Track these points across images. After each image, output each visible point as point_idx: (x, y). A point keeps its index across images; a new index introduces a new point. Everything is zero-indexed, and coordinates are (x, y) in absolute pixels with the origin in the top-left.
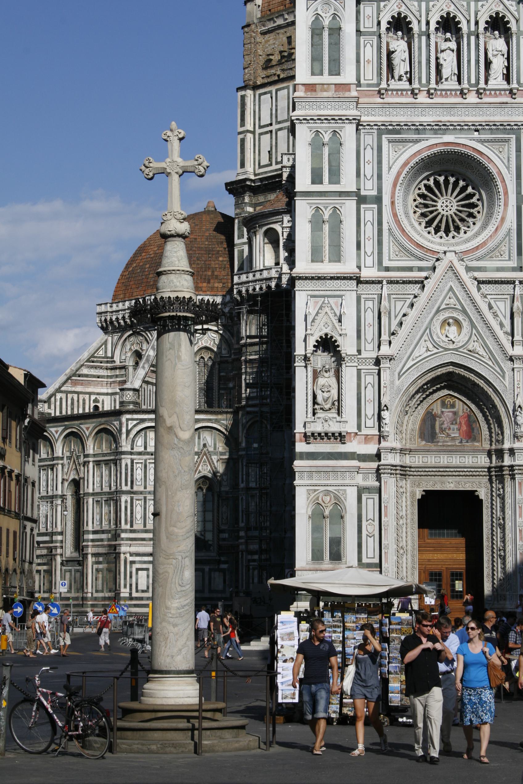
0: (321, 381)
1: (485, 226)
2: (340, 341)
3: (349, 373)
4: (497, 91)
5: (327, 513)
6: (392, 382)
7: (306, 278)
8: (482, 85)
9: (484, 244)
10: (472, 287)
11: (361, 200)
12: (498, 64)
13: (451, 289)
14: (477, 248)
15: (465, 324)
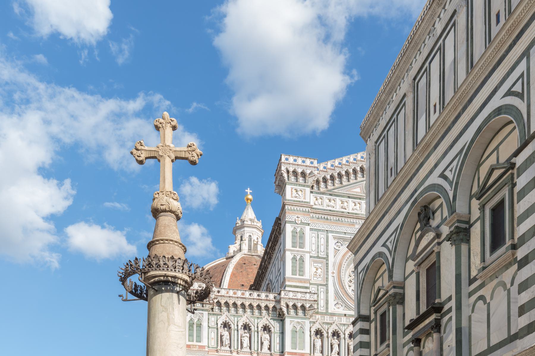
8: (259, 350)
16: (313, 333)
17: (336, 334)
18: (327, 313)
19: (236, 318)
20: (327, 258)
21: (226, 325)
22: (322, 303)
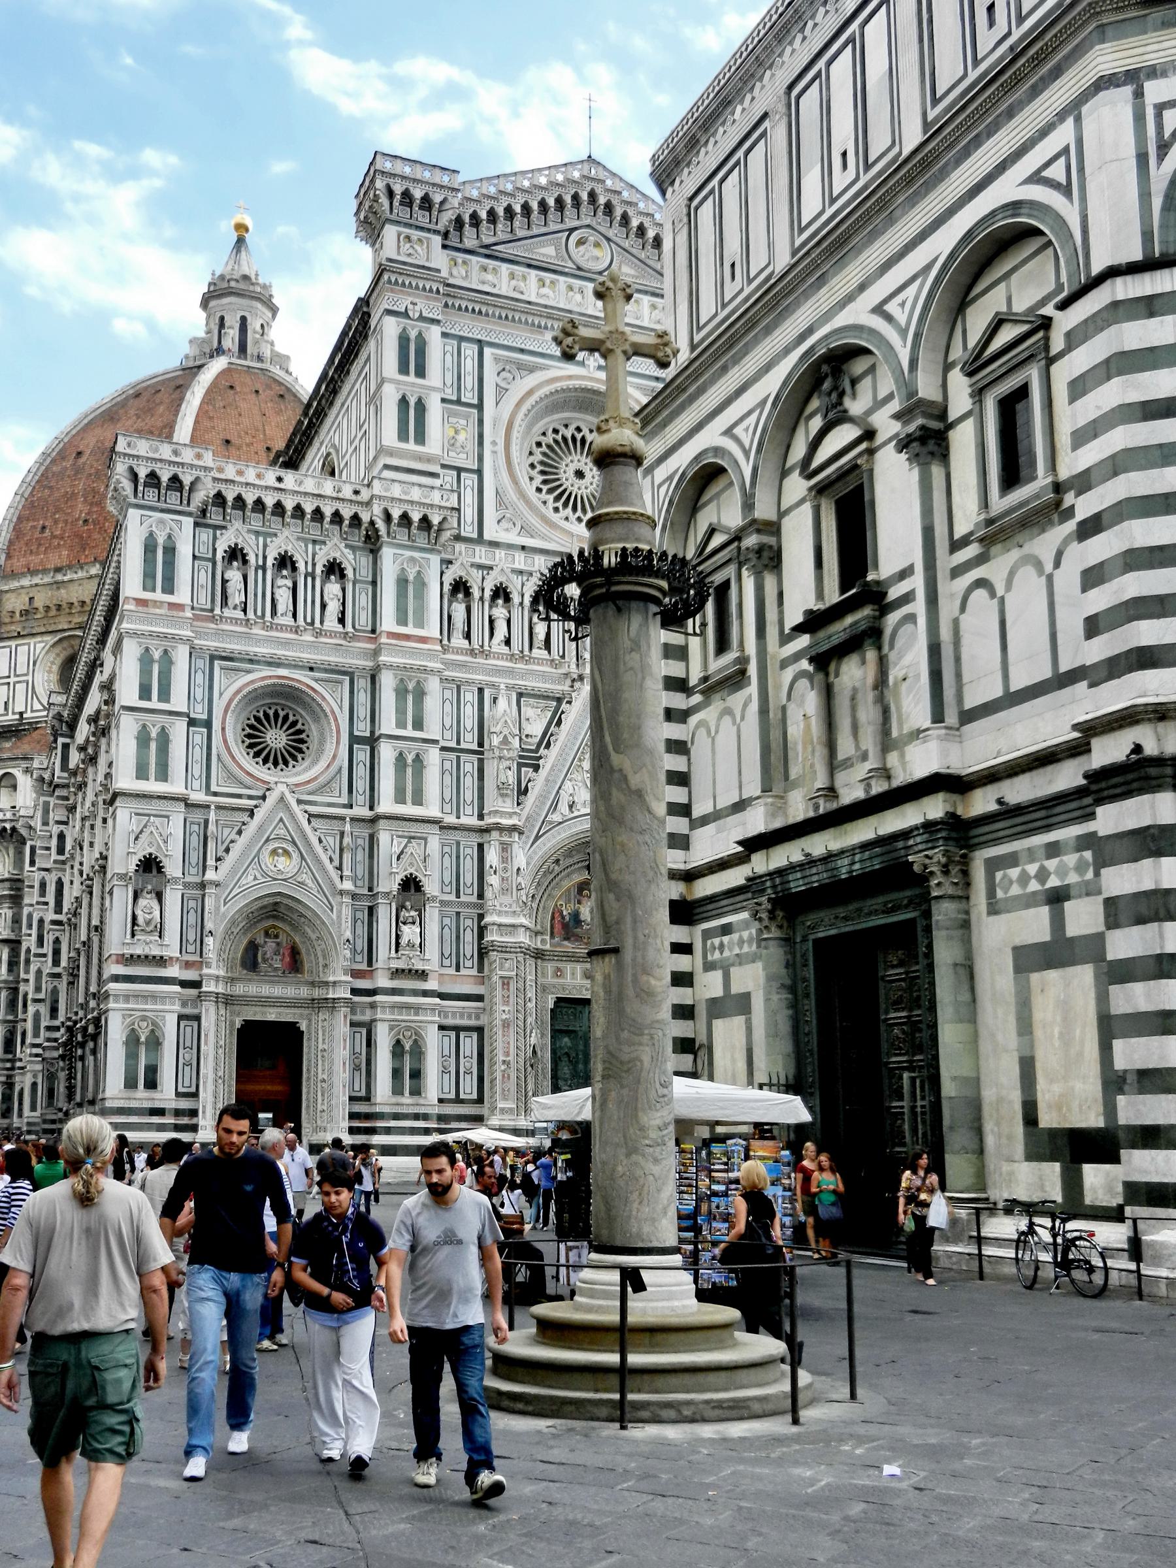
0: (142, 902)
1: (315, 762)
2: (166, 862)
3: (173, 897)
4: (332, 634)
5: (143, 1039)
6: (217, 908)
7: (130, 795)
9: (316, 778)
10: (303, 819)
11: (192, 723)
12: (333, 607)
13: (281, 820)
14: (308, 782)
15: (295, 855)
16: (447, 587)
17: (501, 593)
18: (480, 540)
19: (261, 539)
20: (480, 407)
21: (235, 554)
22: (469, 513)
